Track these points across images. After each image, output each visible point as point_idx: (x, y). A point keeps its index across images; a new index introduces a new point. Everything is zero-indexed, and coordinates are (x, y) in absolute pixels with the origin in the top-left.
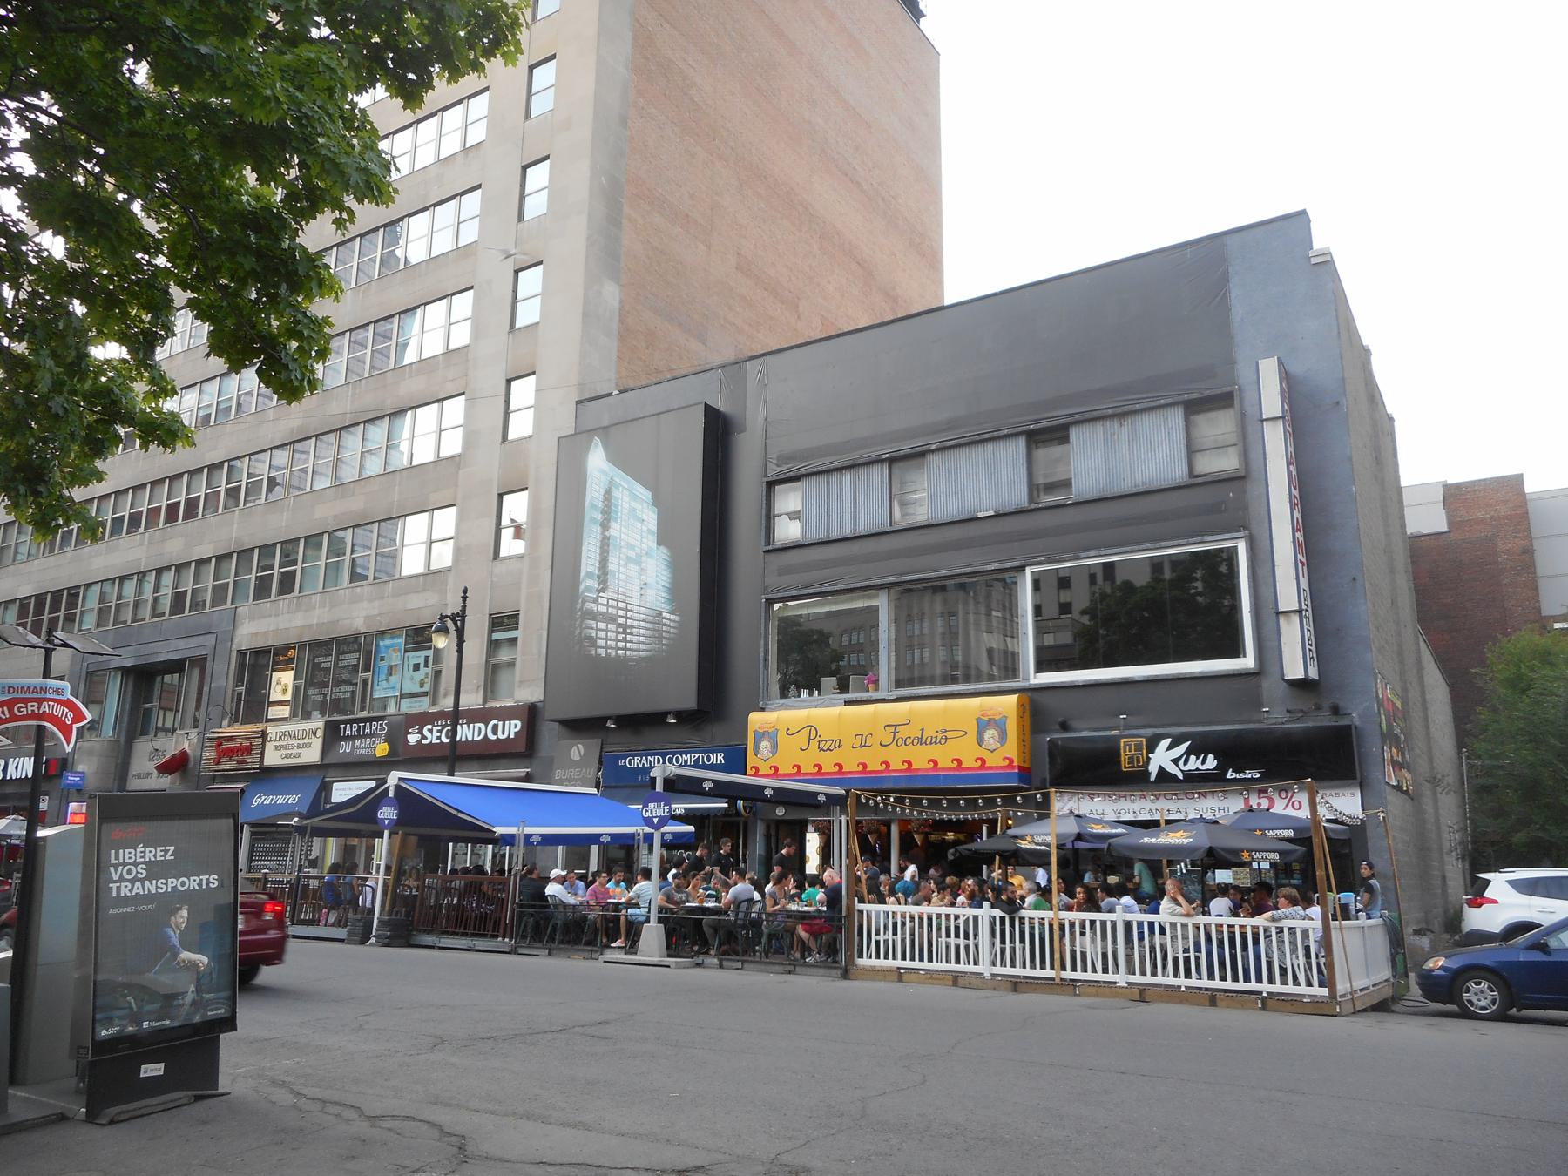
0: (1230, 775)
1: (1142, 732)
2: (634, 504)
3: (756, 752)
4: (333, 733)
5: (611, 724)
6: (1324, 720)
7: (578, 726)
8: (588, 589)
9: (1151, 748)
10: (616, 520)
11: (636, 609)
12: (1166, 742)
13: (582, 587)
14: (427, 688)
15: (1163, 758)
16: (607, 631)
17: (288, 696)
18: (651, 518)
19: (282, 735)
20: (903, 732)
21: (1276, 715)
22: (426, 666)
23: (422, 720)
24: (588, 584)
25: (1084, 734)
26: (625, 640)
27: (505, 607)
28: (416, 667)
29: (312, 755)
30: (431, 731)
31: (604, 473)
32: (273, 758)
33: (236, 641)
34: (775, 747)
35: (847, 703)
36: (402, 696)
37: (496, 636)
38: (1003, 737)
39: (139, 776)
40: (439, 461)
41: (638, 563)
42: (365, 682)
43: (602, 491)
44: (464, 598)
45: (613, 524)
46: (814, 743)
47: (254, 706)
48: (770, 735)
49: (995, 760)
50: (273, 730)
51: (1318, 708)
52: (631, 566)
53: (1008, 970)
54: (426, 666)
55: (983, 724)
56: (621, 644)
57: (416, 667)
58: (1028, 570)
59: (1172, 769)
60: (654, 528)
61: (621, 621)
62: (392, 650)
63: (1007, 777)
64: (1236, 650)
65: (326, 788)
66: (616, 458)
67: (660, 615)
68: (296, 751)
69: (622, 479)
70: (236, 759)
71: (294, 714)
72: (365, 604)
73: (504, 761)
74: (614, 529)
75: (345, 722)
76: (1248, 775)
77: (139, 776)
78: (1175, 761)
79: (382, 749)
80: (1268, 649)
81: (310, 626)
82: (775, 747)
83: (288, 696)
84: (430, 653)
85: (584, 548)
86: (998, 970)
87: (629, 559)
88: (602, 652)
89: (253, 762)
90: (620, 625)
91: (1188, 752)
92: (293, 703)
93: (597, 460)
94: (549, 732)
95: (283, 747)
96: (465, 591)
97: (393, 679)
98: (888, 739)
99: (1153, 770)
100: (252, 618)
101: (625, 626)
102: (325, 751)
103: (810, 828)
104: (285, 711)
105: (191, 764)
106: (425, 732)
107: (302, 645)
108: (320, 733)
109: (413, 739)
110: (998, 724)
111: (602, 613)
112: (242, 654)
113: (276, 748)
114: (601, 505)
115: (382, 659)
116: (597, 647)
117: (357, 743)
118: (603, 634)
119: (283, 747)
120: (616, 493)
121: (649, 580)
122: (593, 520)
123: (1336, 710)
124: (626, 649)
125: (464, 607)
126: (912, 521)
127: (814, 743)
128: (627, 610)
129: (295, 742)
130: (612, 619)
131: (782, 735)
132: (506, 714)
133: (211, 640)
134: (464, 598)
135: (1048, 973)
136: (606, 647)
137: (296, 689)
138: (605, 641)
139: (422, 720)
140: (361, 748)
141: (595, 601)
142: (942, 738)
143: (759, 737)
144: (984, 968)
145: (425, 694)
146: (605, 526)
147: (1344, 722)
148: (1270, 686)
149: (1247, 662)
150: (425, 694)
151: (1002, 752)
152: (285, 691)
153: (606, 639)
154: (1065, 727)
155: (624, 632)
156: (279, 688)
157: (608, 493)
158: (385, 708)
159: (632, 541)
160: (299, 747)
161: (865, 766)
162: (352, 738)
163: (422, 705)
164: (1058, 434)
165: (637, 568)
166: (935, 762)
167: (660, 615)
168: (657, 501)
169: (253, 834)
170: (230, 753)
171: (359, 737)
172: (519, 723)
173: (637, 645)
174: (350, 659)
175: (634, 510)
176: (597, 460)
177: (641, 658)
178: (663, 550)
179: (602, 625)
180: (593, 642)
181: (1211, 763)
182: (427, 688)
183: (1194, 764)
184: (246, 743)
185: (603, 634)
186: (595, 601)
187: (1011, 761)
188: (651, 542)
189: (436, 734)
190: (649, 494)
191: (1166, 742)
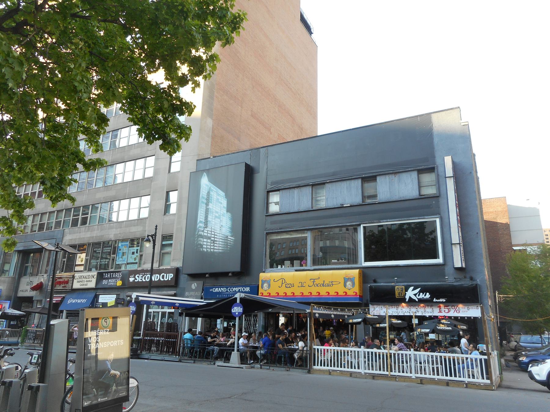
0: (435, 300)
1: (403, 284)
2: (218, 197)
4: (100, 277)
6: (466, 283)
7: (194, 276)
8: (200, 227)
9: (406, 290)
10: (211, 203)
11: (218, 235)
12: (412, 288)
13: (198, 226)
14: (137, 261)
15: (410, 293)
16: (207, 242)
17: (83, 263)
18: (224, 202)
19: (80, 277)
20: (317, 282)
21: (450, 279)
22: (137, 253)
23: (135, 272)
24: (200, 225)
25: (382, 284)
26: (214, 246)
27: (168, 232)
28: (133, 253)
29: (92, 284)
30: (138, 277)
31: (207, 186)
32: (76, 285)
33: (64, 241)
34: (269, 286)
35: (296, 271)
36: (128, 264)
37: (164, 243)
38: (353, 284)
39: (23, 291)
40: (144, 179)
41: (219, 218)
43: (206, 192)
44: (156, 229)
45: (210, 204)
47: (70, 266)
48: (268, 282)
49: (350, 293)
50: (77, 275)
51: (465, 277)
53: (371, 371)
54: (137, 253)
55: (346, 280)
56: (212, 247)
57: (133, 253)
58: (362, 226)
59: (414, 297)
60: (226, 206)
61: (212, 239)
62: (123, 247)
63: (355, 299)
64: (436, 256)
65: (96, 297)
66: (211, 180)
67: (227, 237)
68: (86, 283)
69: (214, 188)
70: (62, 285)
71: (85, 269)
72: (114, 229)
73: (166, 289)
74: (211, 206)
75: (105, 273)
76: (441, 300)
77: (23, 291)
78: (415, 295)
79: (119, 283)
80: (448, 256)
81: (93, 237)
82: (269, 286)
83: (83, 263)
84: (139, 248)
85: (199, 212)
86: (367, 371)
87: (216, 217)
88: (205, 250)
89: (69, 286)
90: (212, 240)
91: (420, 292)
92: (85, 265)
93: (205, 181)
94: (183, 278)
95: (81, 281)
96: (156, 226)
97: (124, 257)
98: (311, 284)
99: (407, 297)
100: (70, 233)
101: (214, 241)
102: (97, 283)
103: (281, 315)
104: (82, 268)
105: (44, 287)
106: (136, 277)
107: (89, 244)
108: (95, 277)
109: (131, 279)
110: (352, 280)
111: (205, 236)
113: (78, 282)
114: (206, 197)
115: (120, 250)
117: (110, 280)
118: (205, 243)
119: (81, 281)
120: (211, 193)
121: (223, 225)
122: (203, 202)
123: (472, 279)
124: (214, 249)
125: (156, 232)
126: (319, 207)
128: (215, 235)
129: (86, 280)
130: (209, 238)
131: (272, 283)
132: (167, 271)
134: (156, 229)
135: (386, 373)
136: (207, 248)
137: (87, 260)
138: (206, 246)
139: (135, 272)
140: (111, 282)
141: (203, 231)
142: (331, 284)
143: (264, 282)
144: (362, 371)
145: (136, 263)
146: (207, 204)
147: (474, 283)
148: (449, 270)
149: (440, 260)
150: (136, 263)
151: (353, 290)
152: (82, 261)
153: (207, 245)
154: (375, 281)
155: (214, 243)
156: (80, 259)
157: (208, 193)
158: (120, 268)
159: (217, 210)
160: (87, 281)
161: (303, 293)
162: (108, 279)
163: (135, 267)
164: (373, 178)
165: (219, 220)
166: (329, 293)
167: (227, 237)
168: (227, 196)
169: (67, 313)
171: (110, 278)
172: (172, 275)
173: (218, 247)
174: (107, 250)
175: (218, 199)
176: (205, 181)
177: (220, 253)
179: (205, 240)
180: (202, 246)
181: (428, 296)
182: (137, 261)
183: (422, 296)
184: (66, 279)
185: (205, 243)
186: (203, 231)
187: (356, 293)
189: (140, 278)
190: (224, 194)
191: (412, 288)
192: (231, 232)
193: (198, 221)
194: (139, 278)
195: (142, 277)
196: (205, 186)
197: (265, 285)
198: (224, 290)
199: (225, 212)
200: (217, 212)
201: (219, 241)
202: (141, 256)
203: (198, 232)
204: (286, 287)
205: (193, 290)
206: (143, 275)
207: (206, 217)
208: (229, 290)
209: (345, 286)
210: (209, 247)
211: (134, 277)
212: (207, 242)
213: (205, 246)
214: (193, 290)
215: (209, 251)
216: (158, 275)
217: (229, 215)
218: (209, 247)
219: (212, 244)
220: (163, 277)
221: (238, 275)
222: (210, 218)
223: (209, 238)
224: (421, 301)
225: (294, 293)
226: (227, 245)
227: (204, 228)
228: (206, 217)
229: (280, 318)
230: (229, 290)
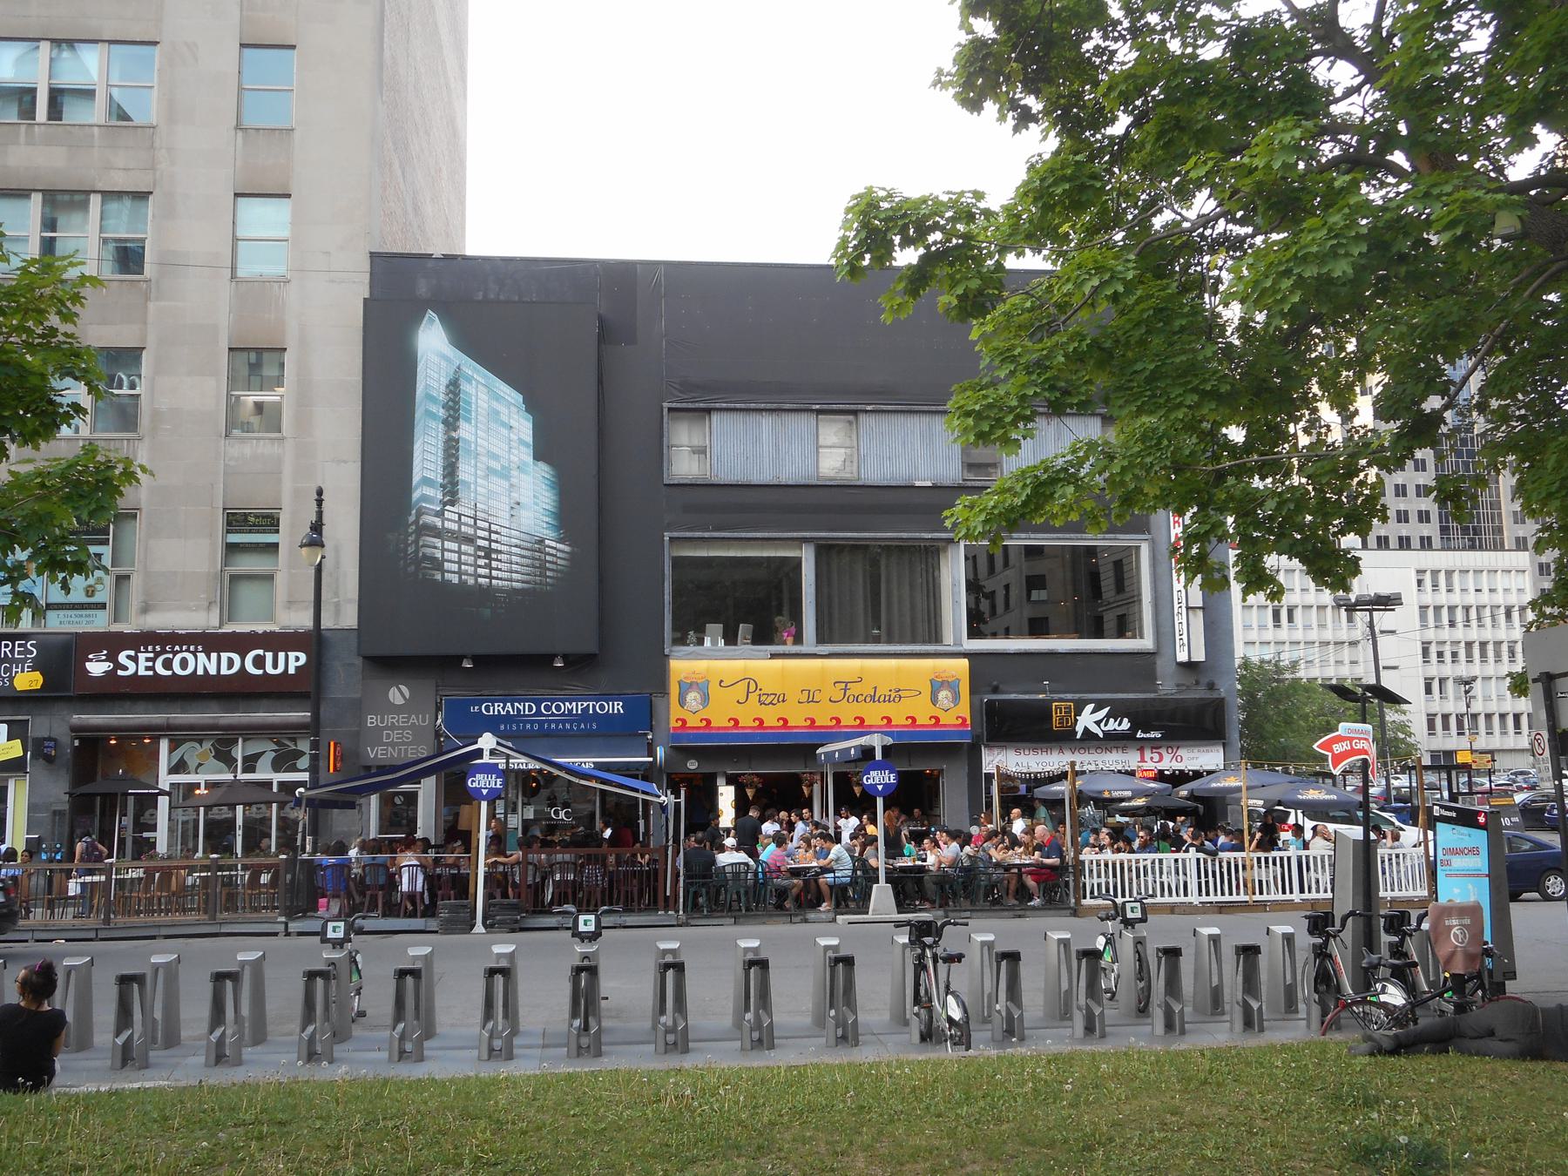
0: (1139, 735)
1: (1069, 696)
2: (495, 404)
3: (682, 702)
5: (467, 665)
6: (1199, 694)
8: (425, 498)
9: (1079, 712)
10: (468, 420)
11: (504, 531)
12: (1090, 707)
13: (416, 495)
15: (1088, 720)
16: (459, 552)
18: (524, 427)
20: (855, 689)
21: (1167, 686)
25: (1013, 696)
27: (254, 499)
30: (135, 659)
34: (706, 699)
35: (774, 656)
37: (234, 538)
38: (956, 698)
41: (507, 477)
43: (444, 381)
44: (320, 502)
45: (462, 423)
46: (754, 697)
49: (948, 719)
51: (1197, 683)
52: (494, 479)
53: (1212, 898)
55: (937, 686)
58: (962, 544)
59: (1095, 729)
60: (530, 440)
61: (481, 543)
63: (961, 734)
67: (541, 541)
69: (470, 367)
73: (265, 702)
74: (465, 431)
76: (1152, 735)
78: (1098, 723)
79: (28, 680)
80: (1164, 631)
82: (706, 699)
86: (1204, 898)
87: (490, 471)
88: (455, 579)
91: (1108, 716)
93: (433, 343)
96: (320, 492)
99: (1079, 729)
101: (488, 553)
103: (721, 781)
110: (953, 686)
111: (449, 531)
114: (442, 397)
116: (444, 572)
118: (455, 557)
120: (464, 386)
121: (522, 500)
123: (1211, 686)
124: (491, 577)
125: (320, 514)
127: (754, 697)
128: (491, 532)
130: (470, 540)
131: (714, 689)
134: (320, 502)
135: (1242, 897)
136: (460, 573)
138: (457, 564)
139: (112, 644)
141: (440, 514)
142: (896, 696)
143: (685, 687)
144: (1194, 898)
145: (103, 606)
146: (451, 423)
147: (1215, 696)
148: (1163, 667)
149: (1146, 643)
150: (103, 606)
151: (955, 712)
153: (459, 563)
154: (995, 690)
155: (488, 556)
157: (454, 386)
159: (495, 450)
161: (813, 721)
163: (99, 623)
165: (505, 484)
166: (889, 720)
167: (541, 541)
168: (531, 405)
172: (303, 658)
173: (509, 573)
175: (498, 413)
176: (433, 343)
177: (515, 590)
178: (543, 466)
179: (454, 546)
180: (438, 565)
181: (1126, 725)
183: (1112, 725)
185: (455, 557)
186: (440, 514)
187: (964, 720)
188: (527, 455)
190: (520, 398)
191: (1090, 707)
192: (557, 528)
193: (416, 479)
194: (135, 664)
195: (153, 660)
196: (436, 359)
197: (693, 697)
198: (525, 708)
199: (531, 459)
200: (495, 457)
201: (510, 554)
202: (122, 579)
203: (420, 513)
204: (762, 703)
205: (398, 709)
206: (157, 655)
207: (451, 469)
208: (548, 708)
209: (934, 701)
210: (471, 570)
211: (112, 658)
212: (459, 552)
213: (455, 567)
214: (398, 709)
215: (471, 581)
216: (236, 658)
217: (544, 470)
218: (471, 570)
219: (481, 562)
220: (260, 662)
221: (582, 667)
222: (465, 472)
223: (470, 540)
224: (1109, 736)
225: (786, 721)
226: (543, 568)
227: (445, 504)
228: (451, 469)
229: (721, 789)
230: (548, 708)
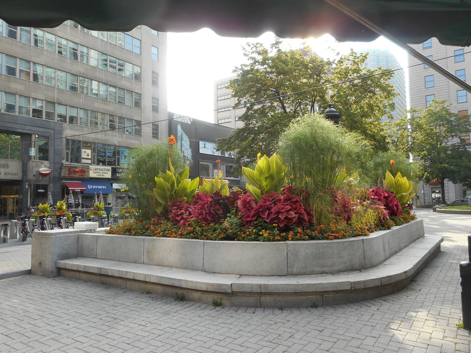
4: (114, 171)
32: (92, 174)
42: (118, 159)
47: (77, 159)
68: (102, 174)
69: (183, 133)
81: (98, 139)
89: (86, 176)
97: (126, 159)
100: (71, 129)
108: (110, 170)
112: (68, 140)
129: (102, 172)
133: (52, 132)
146: (181, 141)
152: (88, 155)
160: (103, 173)
170: (75, 172)
188: (189, 147)
